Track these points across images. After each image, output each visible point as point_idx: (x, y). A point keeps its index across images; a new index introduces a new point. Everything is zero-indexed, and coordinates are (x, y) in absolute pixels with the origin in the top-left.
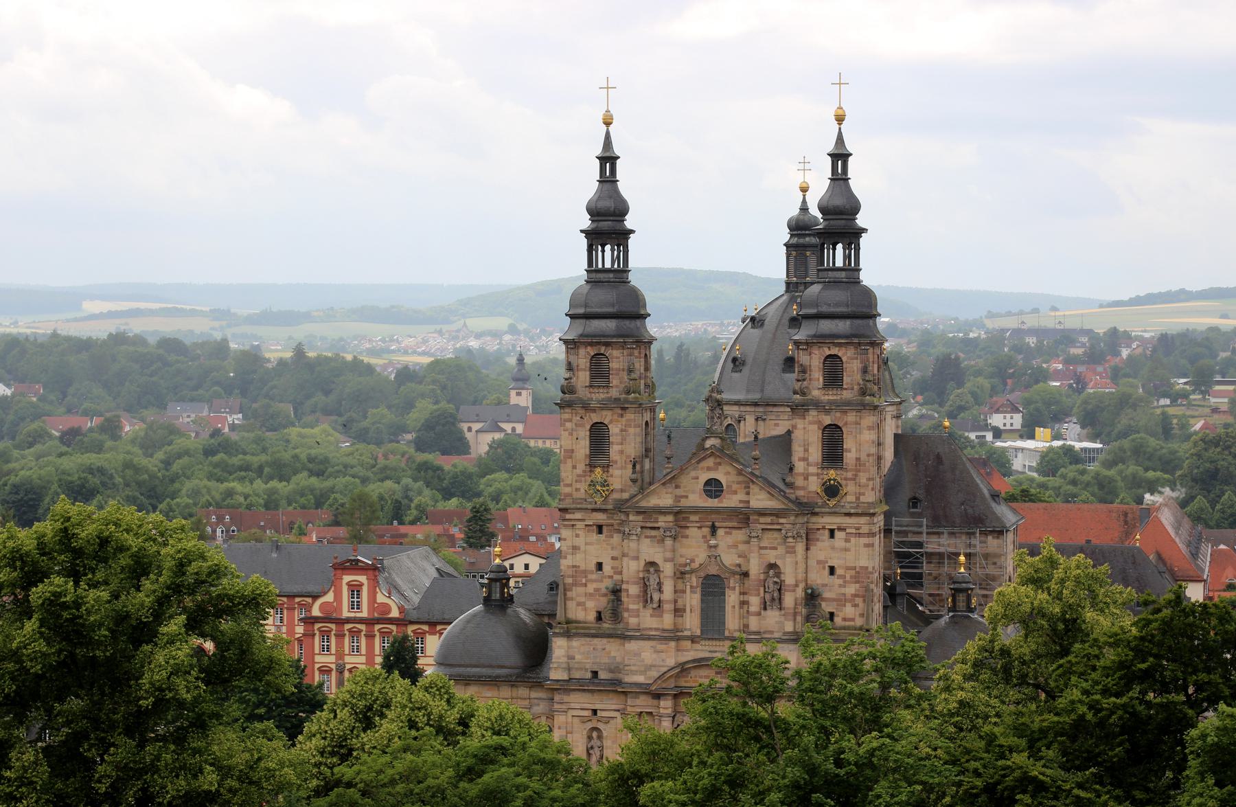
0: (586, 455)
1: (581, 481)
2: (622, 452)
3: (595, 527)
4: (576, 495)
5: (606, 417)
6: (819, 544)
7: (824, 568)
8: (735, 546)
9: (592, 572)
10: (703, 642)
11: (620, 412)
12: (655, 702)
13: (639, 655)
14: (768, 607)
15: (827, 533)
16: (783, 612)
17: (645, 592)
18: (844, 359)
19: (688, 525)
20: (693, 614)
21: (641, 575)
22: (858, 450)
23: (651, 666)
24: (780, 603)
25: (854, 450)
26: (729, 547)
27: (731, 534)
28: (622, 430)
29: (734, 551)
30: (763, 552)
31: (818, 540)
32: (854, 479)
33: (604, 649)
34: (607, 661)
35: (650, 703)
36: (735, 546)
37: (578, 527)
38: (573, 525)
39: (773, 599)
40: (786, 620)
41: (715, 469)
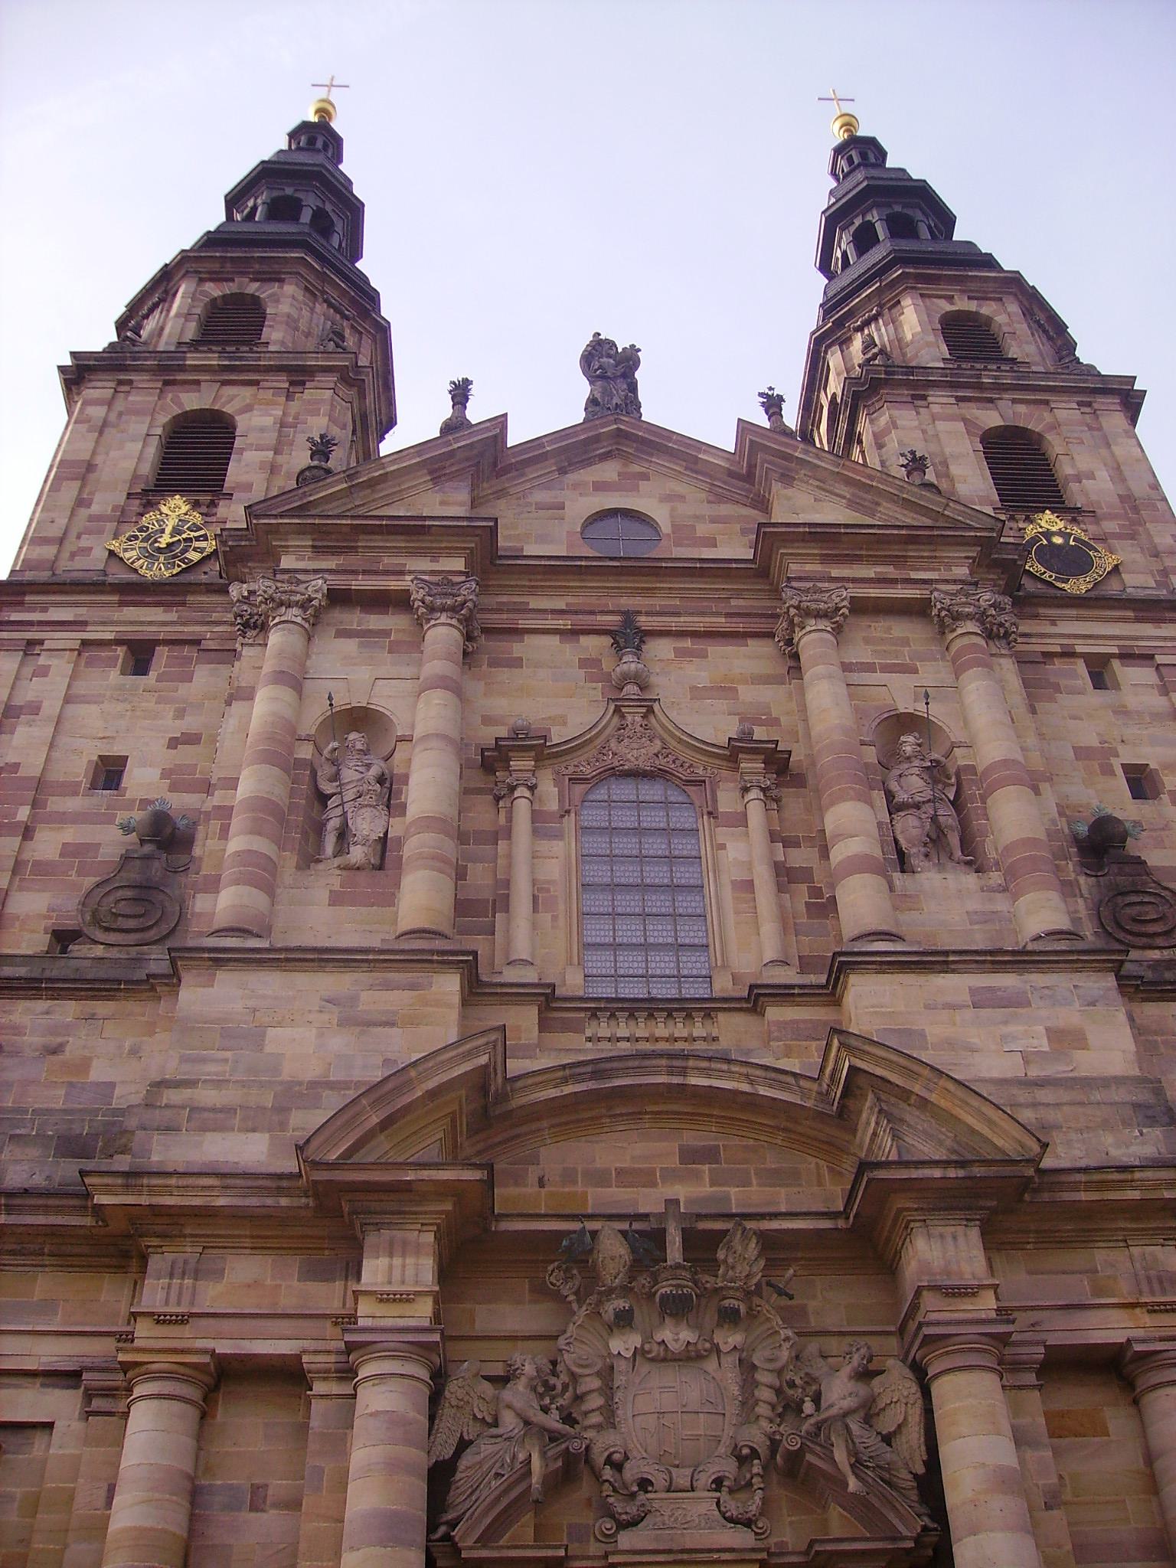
0: (135, 477)
1: (100, 532)
2: (273, 469)
3: (121, 651)
4: (64, 564)
5: (232, 400)
6: (1063, 699)
7: (1108, 771)
8: (725, 690)
9: (72, 790)
10: (604, 1029)
11: (286, 385)
12: (328, 1296)
13: (257, 1038)
14: (914, 861)
15: (1081, 667)
16: (995, 878)
17: (320, 828)
18: (1000, 319)
19: (523, 624)
20: (545, 918)
21: (305, 752)
22: (1118, 472)
23: (314, 1085)
24: (968, 843)
25: (1103, 474)
26: (696, 693)
27: (703, 655)
28: (283, 425)
29: (722, 705)
30: (856, 677)
31: (1057, 688)
32: (1132, 536)
33: (56, 1050)
34: (60, 1105)
35: (287, 1302)
36: (725, 690)
37: (47, 645)
38: (31, 643)
39: (936, 840)
40: (1015, 898)
41: (629, 482)
